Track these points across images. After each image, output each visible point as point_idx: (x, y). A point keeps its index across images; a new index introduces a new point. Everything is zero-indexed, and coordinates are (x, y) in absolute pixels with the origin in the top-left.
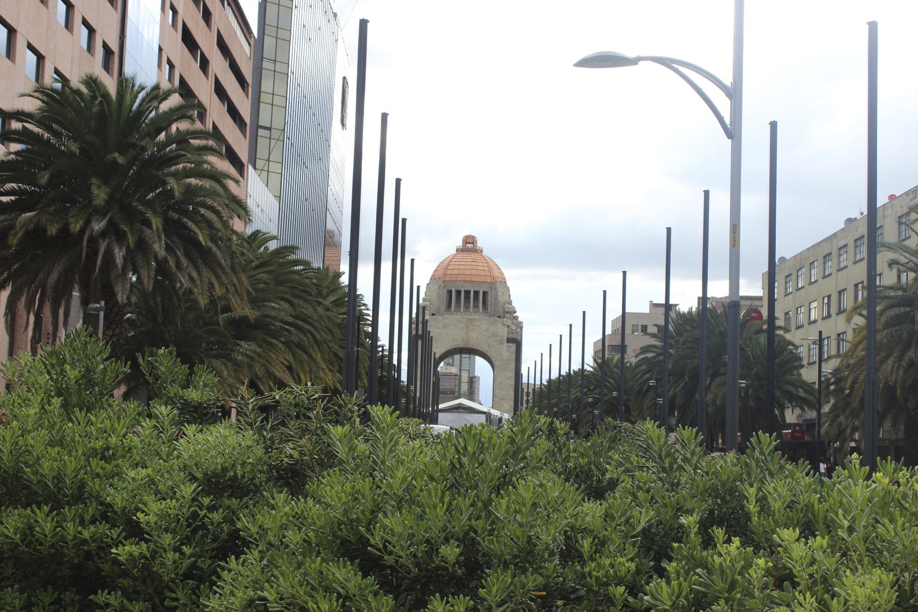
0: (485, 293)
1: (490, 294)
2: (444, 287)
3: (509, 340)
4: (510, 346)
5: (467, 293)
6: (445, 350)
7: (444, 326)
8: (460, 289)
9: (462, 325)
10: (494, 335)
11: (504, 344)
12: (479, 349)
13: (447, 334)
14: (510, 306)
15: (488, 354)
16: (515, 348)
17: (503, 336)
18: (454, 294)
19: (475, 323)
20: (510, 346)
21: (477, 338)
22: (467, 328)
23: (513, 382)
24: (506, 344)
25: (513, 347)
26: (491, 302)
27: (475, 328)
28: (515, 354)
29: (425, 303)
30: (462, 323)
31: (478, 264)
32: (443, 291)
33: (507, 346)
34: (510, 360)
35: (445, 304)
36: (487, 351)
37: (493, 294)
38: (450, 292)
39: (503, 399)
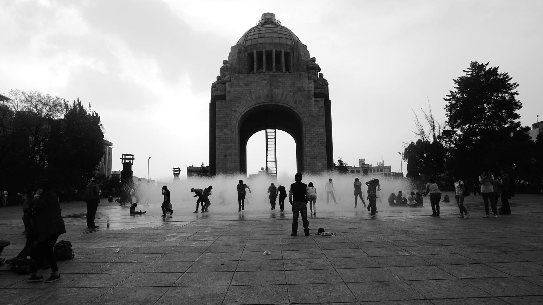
0: (287, 54)
1: (292, 55)
2: (245, 51)
3: (316, 95)
4: (318, 101)
5: (269, 54)
6: (248, 109)
7: (247, 85)
10: (300, 90)
11: (311, 99)
12: (286, 105)
13: (250, 92)
14: (313, 63)
15: (295, 110)
16: (324, 103)
17: (309, 91)
18: (255, 55)
19: (279, 80)
20: (318, 101)
21: (282, 94)
22: (271, 85)
23: (324, 139)
24: (313, 99)
27: (280, 84)
29: (226, 65)
30: (265, 80)
31: (278, 29)
32: (245, 55)
33: (315, 101)
34: (319, 116)
35: (247, 67)
36: (294, 108)
37: (295, 55)
38: (251, 55)
39: (315, 158)
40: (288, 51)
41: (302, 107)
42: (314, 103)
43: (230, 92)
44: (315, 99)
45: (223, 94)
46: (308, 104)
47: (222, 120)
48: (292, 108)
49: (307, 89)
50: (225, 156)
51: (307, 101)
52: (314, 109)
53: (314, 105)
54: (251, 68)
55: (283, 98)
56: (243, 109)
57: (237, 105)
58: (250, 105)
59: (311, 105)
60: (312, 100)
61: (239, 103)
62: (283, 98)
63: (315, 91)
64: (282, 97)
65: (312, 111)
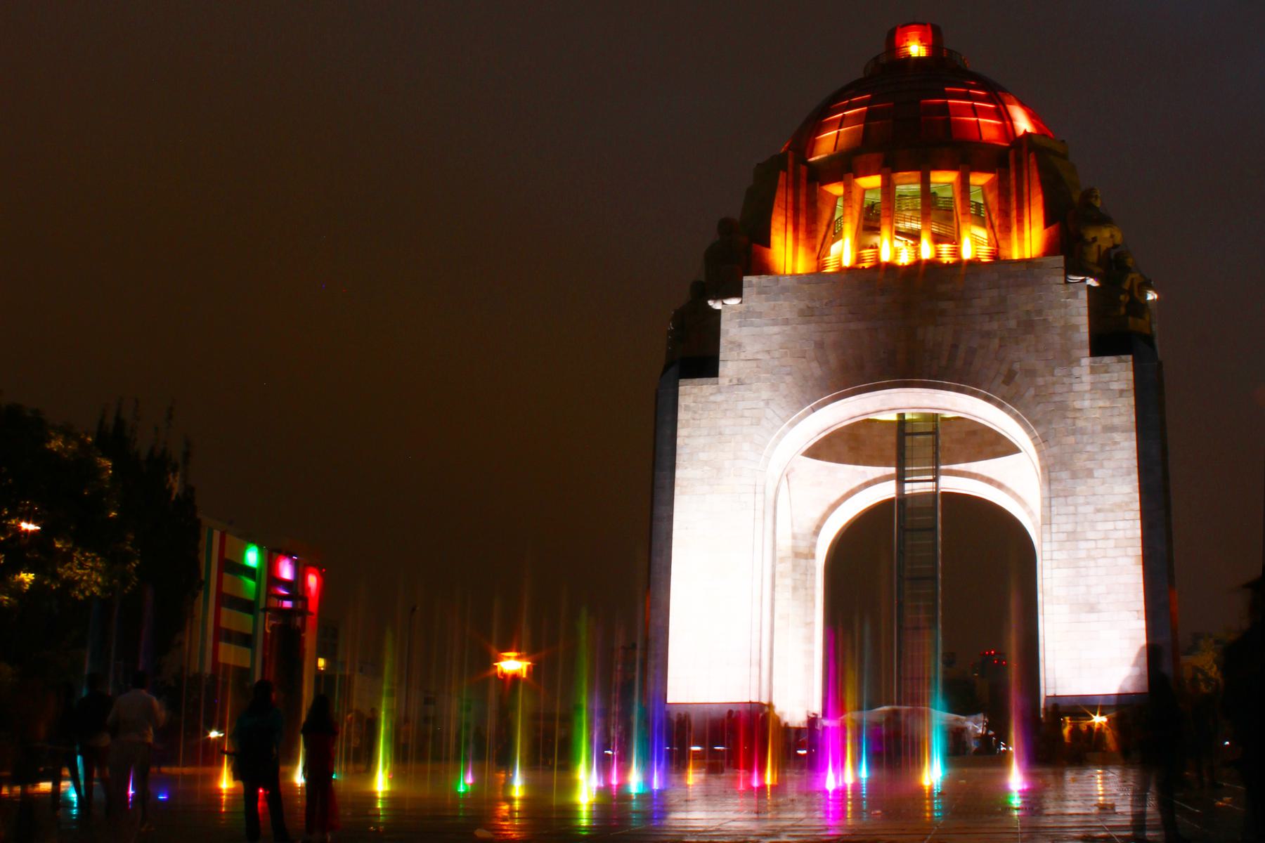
11: (1077, 362)
16: (1131, 375)
24: (1086, 361)
28: (1132, 401)
33: (1093, 370)
41: (1036, 396)
42: (1087, 378)
43: (740, 345)
44: (1091, 358)
46: (1064, 384)
47: (703, 456)
51: (1059, 372)
52: (1087, 403)
53: (1087, 387)
59: (1076, 387)
60: (1079, 365)
65: (1080, 410)
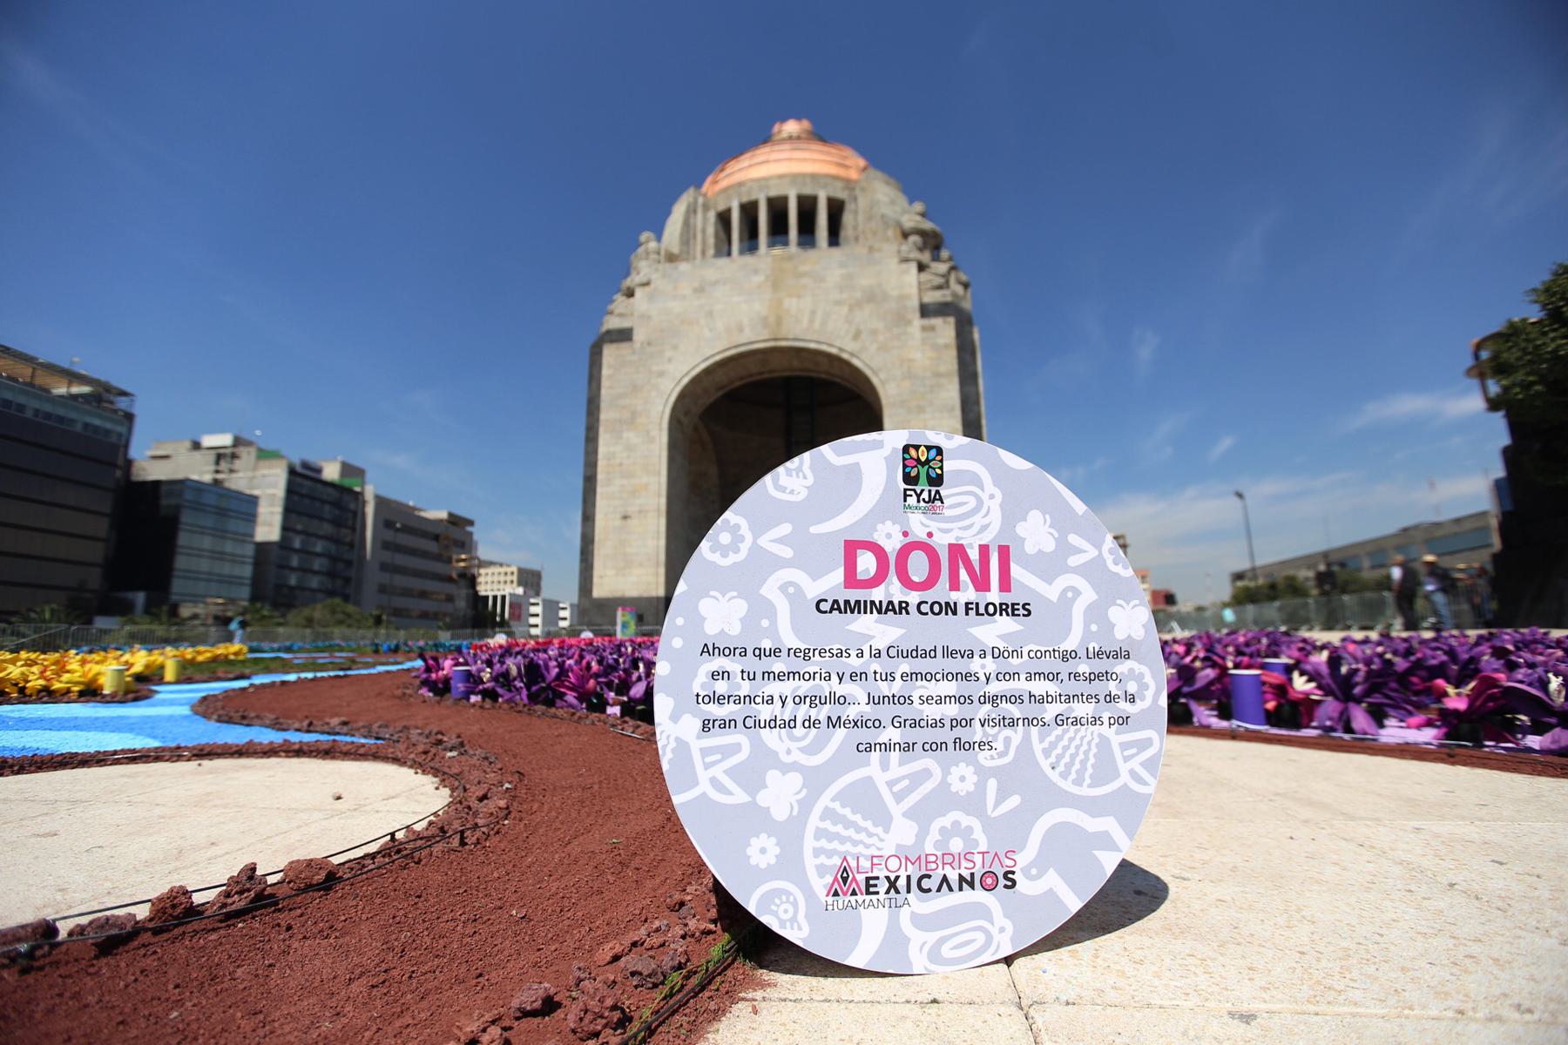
3: (926, 311)
5: (778, 210)
7: (700, 290)
8: (753, 197)
9: (760, 278)
11: (909, 322)
12: (824, 348)
13: (710, 314)
15: (856, 362)
17: (902, 298)
19: (804, 268)
20: (932, 328)
21: (813, 313)
22: (776, 284)
24: (918, 322)
25: (946, 330)
26: (855, 228)
27: (805, 281)
30: (756, 272)
32: (705, 219)
33: (924, 329)
34: (938, 375)
36: (852, 355)
40: (840, 194)
43: (649, 317)
45: (625, 324)
48: (845, 356)
49: (894, 293)
50: (625, 517)
52: (917, 355)
54: (729, 254)
55: (817, 325)
56: (686, 368)
57: (668, 354)
58: (709, 353)
61: (675, 347)
62: (817, 325)
63: (920, 299)
64: (811, 321)
